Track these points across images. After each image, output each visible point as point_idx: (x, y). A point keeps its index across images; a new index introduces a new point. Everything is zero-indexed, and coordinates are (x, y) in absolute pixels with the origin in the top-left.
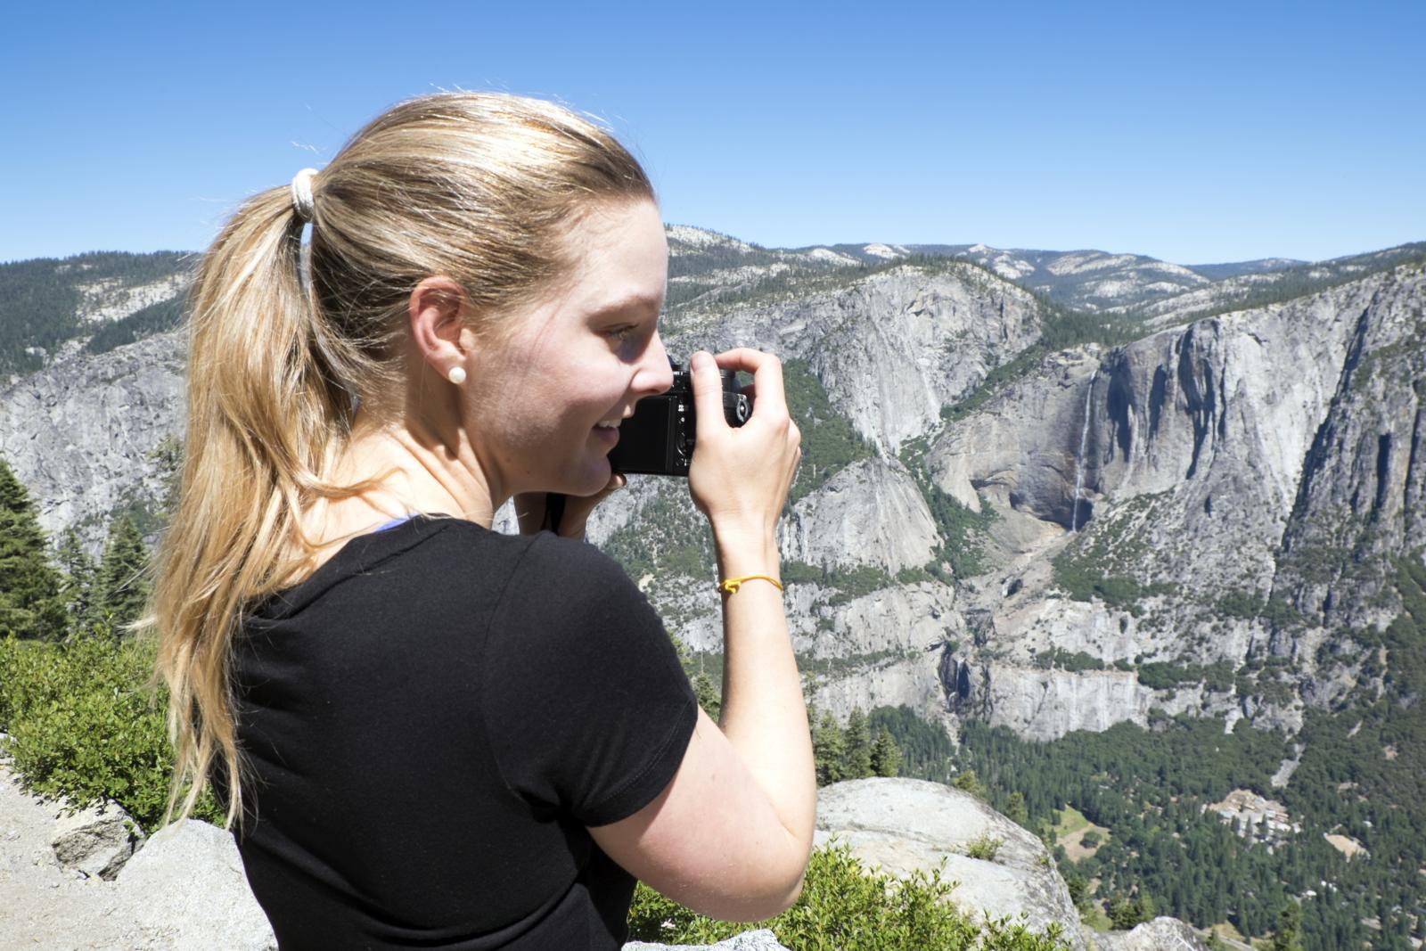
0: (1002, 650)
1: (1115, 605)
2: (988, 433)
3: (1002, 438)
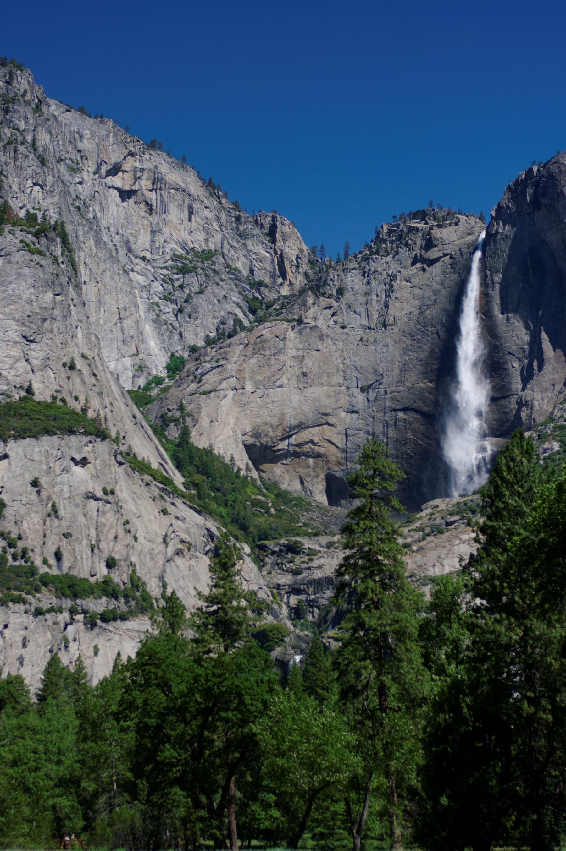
2: (280, 351)
3: (308, 362)
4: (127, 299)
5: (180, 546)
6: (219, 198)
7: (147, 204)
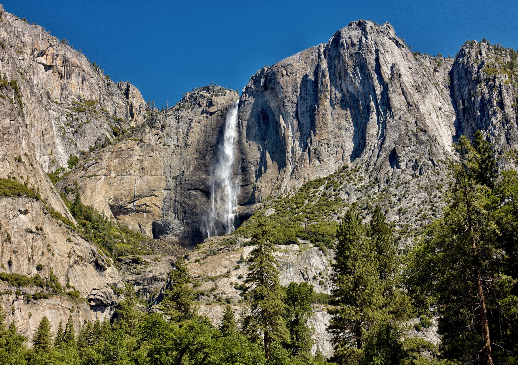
2: (130, 156)
3: (145, 163)
4: (47, 124)
5: (77, 259)
6: (98, 73)
7: (59, 73)
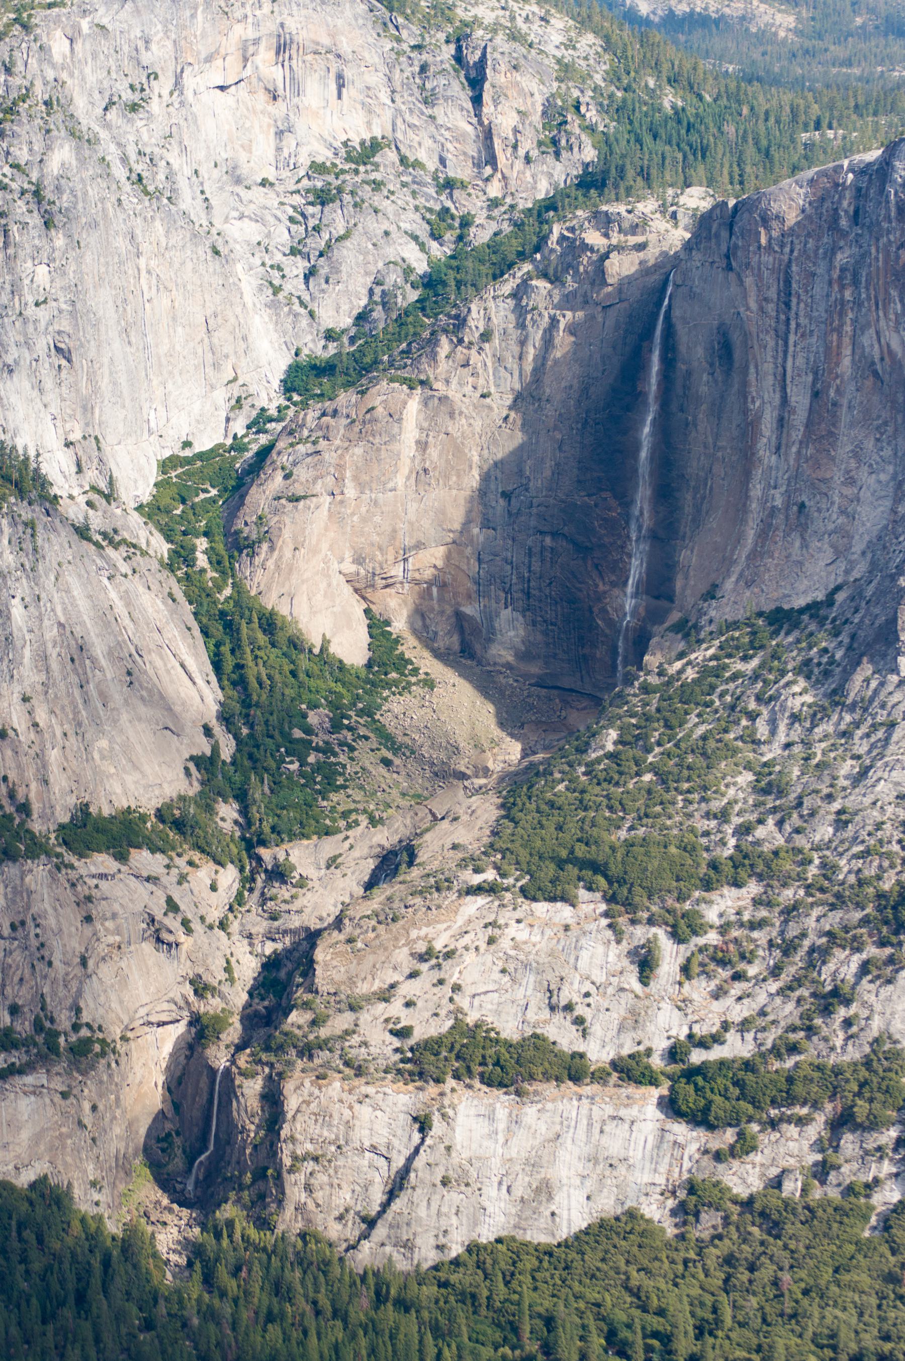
0: (324, 1032)
1: (630, 906)
3: (433, 452)
4: (218, 298)
